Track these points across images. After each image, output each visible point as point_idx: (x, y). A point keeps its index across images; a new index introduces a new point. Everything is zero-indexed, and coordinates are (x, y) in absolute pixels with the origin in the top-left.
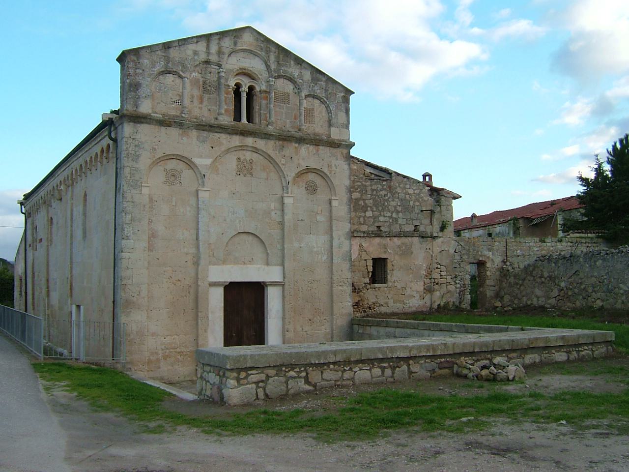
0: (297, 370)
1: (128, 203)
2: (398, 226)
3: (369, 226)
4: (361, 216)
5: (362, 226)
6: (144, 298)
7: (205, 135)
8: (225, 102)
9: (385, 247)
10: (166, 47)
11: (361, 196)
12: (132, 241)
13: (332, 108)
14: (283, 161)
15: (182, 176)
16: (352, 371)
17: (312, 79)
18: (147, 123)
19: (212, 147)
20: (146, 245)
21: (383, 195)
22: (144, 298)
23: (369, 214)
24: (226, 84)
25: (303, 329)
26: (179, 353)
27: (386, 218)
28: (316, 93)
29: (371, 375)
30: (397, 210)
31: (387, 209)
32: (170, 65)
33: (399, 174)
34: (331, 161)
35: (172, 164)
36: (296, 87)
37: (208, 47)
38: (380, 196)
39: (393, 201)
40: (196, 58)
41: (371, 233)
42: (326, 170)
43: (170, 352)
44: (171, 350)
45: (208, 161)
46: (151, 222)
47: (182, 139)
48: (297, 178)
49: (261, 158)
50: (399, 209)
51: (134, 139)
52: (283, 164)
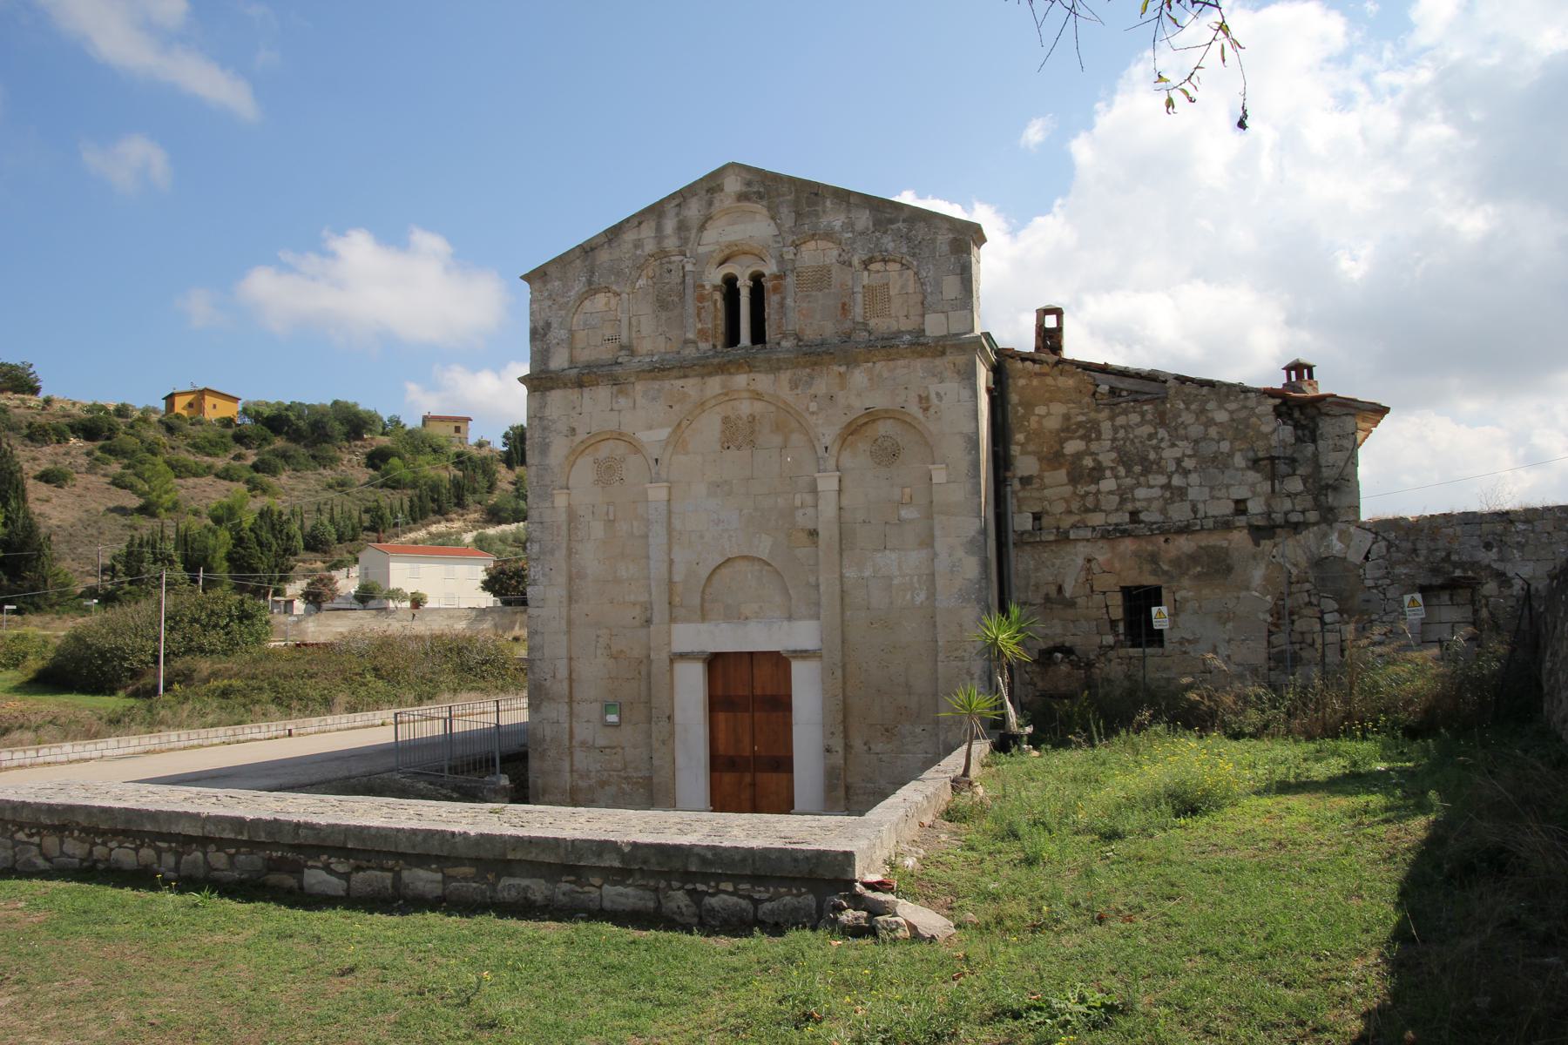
0: (27, 831)
1: (536, 525)
2: (1187, 506)
3: (1108, 513)
4: (1087, 493)
5: (1090, 515)
6: (561, 681)
7: (657, 387)
8: (699, 315)
9: (1154, 558)
10: (588, 249)
11: (1087, 445)
12: (542, 588)
13: (928, 272)
14: (813, 407)
15: (623, 466)
16: (106, 846)
17: (874, 225)
18: (559, 388)
19: (671, 407)
20: (564, 593)
21: (1145, 436)
22: (561, 681)
23: (1108, 484)
25: (870, 749)
26: (625, 778)
27: (1153, 490)
28: (886, 251)
29: (138, 861)
30: (1184, 469)
31: (1155, 467)
32: (595, 279)
33: (1182, 380)
34: (927, 387)
35: (605, 450)
37: (659, 228)
38: (1136, 441)
39: (1173, 445)
40: (638, 252)
41: (1111, 528)
42: (914, 409)
43: (610, 776)
44: (612, 773)
45: (663, 433)
46: (576, 553)
47: (617, 402)
48: (851, 434)
49: (772, 408)
50: (1189, 464)
51: (540, 418)
52: (813, 413)
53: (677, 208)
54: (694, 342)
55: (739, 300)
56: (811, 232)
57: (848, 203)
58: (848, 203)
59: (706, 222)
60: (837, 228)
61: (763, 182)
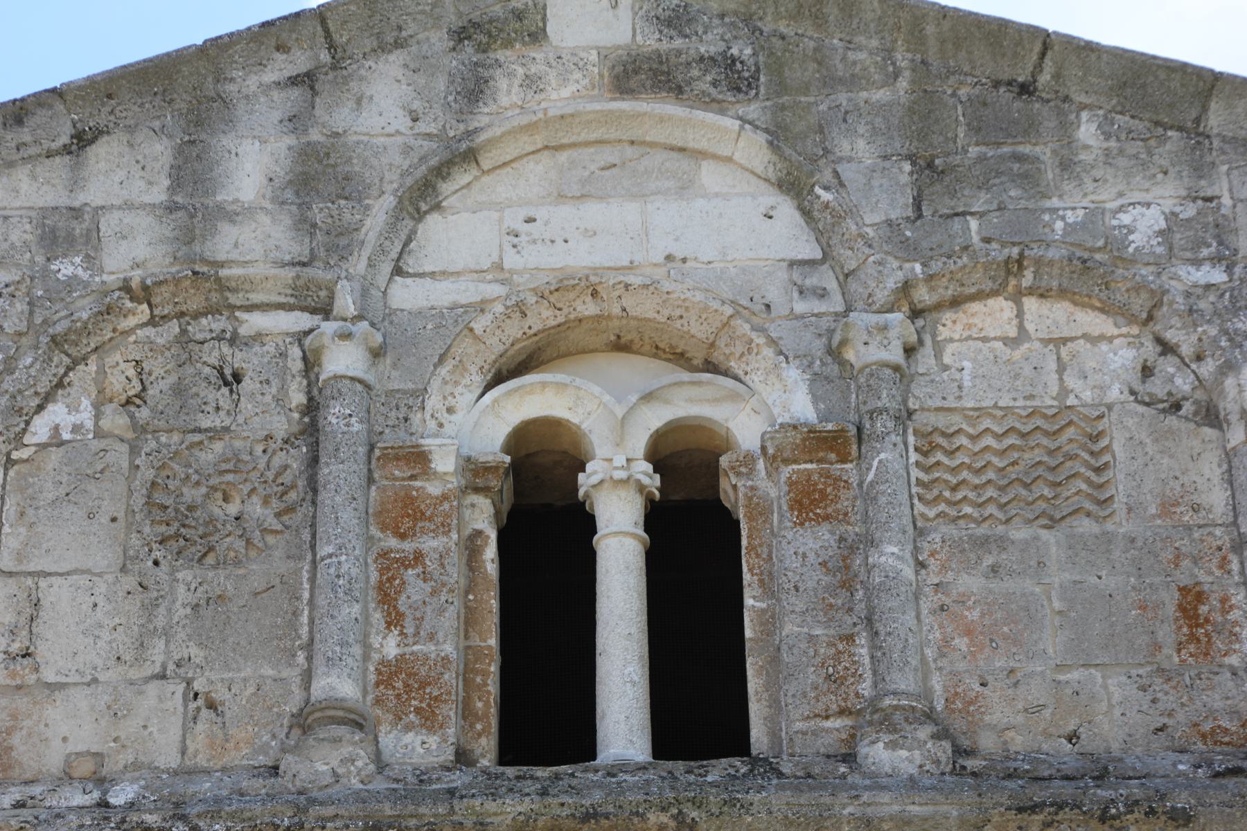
8: (387, 595)
24: (390, 439)
36: (1167, 348)
40: (66, 268)
53: (295, 93)
54: (357, 722)
55: (590, 558)
56: (998, 253)
57: (1197, 134)
58: (1197, 134)
59: (442, 171)
60: (1137, 239)
61: (748, 19)
